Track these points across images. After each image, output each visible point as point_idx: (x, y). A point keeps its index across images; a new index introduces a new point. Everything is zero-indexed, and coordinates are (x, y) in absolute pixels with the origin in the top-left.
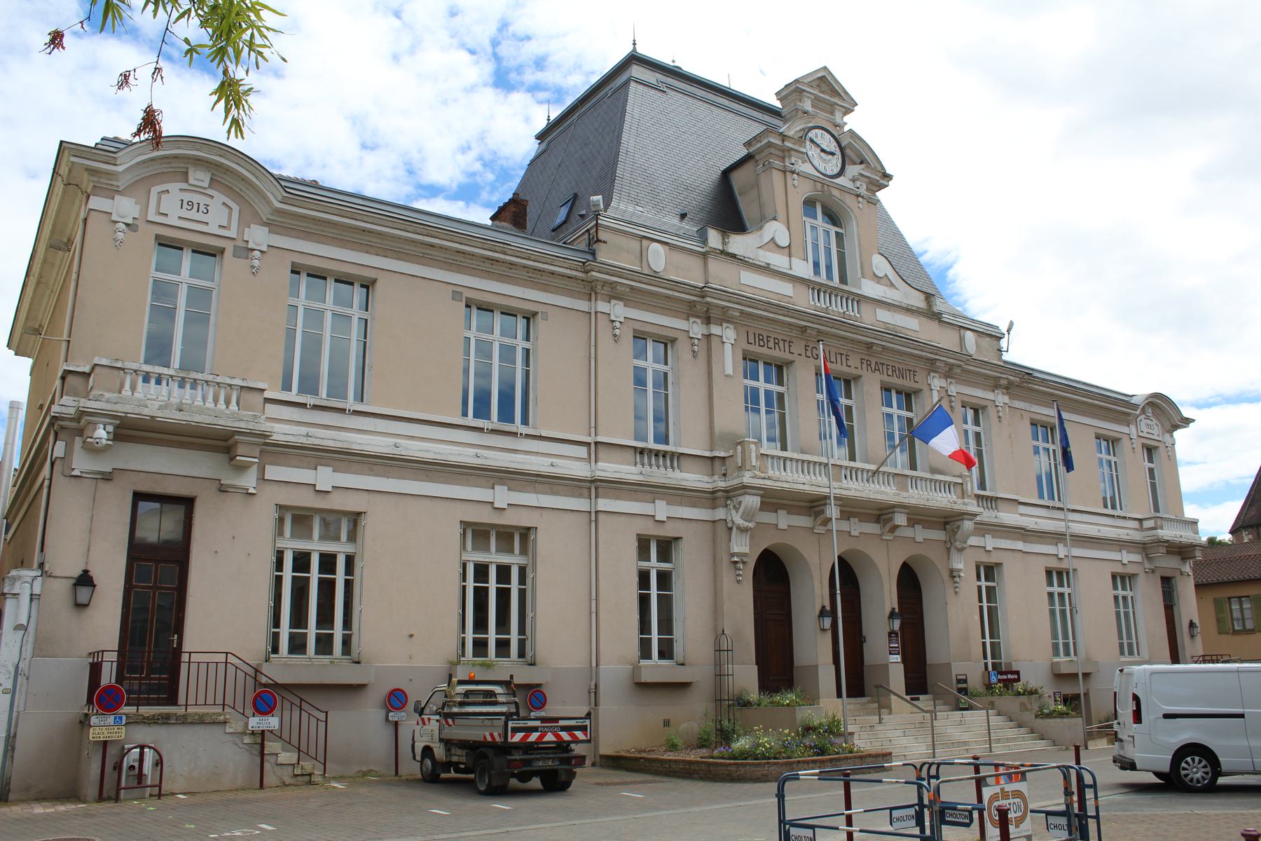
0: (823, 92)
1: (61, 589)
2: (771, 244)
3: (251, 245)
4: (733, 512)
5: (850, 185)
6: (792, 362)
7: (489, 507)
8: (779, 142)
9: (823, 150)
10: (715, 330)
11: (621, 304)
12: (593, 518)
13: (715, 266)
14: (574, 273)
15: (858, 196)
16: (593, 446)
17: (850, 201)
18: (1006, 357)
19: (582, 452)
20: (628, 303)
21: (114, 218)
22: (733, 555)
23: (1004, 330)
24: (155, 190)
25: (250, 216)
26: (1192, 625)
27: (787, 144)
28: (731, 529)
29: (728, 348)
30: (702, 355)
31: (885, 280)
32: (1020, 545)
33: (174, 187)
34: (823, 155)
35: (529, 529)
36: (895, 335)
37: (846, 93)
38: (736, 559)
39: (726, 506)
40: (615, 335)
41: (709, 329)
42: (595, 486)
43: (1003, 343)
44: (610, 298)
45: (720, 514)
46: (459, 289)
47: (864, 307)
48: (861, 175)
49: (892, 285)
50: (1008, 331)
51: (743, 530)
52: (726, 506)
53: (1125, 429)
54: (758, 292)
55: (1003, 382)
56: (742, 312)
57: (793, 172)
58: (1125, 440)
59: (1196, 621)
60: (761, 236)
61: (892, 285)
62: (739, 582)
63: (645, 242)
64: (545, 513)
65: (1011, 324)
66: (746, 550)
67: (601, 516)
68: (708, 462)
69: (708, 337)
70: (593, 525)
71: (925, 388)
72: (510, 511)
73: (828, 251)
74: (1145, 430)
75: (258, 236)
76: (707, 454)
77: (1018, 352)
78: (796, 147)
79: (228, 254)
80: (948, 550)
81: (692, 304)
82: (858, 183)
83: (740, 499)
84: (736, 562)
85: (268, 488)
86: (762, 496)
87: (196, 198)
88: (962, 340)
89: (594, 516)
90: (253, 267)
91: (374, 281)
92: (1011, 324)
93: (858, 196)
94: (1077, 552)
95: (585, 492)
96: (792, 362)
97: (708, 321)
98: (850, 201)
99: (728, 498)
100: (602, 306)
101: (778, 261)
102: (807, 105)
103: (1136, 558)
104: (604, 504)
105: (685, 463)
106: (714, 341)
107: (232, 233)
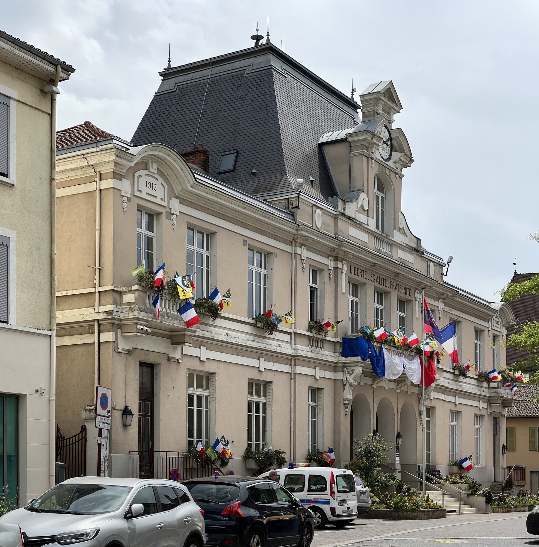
1: (117, 415)
3: (173, 212)
4: (348, 375)
6: (365, 284)
7: (257, 370)
10: (340, 265)
11: (305, 248)
12: (293, 377)
13: (342, 224)
14: (291, 230)
16: (293, 334)
18: (445, 278)
19: (287, 338)
20: (309, 249)
21: (123, 194)
22: (345, 400)
23: (446, 262)
24: (137, 174)
25: (172, 194)
26: (504, 446)
28: (344, 385)
29: (344, 275)
30: (333, 279)
32: (443, 396)
33: (143, 172)
35: (267, 382)
36: (403, 265)
38: (347, 402)
39: (343, 371)
40: (303, 268)
41: (337, 264)
42: (293, 360)
43: (444, 270)
44: (302, 245)
45: (340, 375)
46: (246, 239)
47: (394, 248)
50: (449, 262)
51: (351, 385)
52: (343, 371)
53: (485, 324)
54: (357, 241)
55: (445, 296)
56: (353, 255)
58: (486, 332)
59: (505, 445)
60: (357, 204)
62: (346, 415)
63: (314, 208)
64: (276, 374)
65: (451, 258)
66: (351, 398)
67: (297, 376)
68: (333, 344)
69: (336, 268)
70: (293, 380)
71: (414, 299)
72: (269, 373)
73: (378, 208)
74: (495, 325)
75: (176, 206)
76: (334, 340)
77: (453, 278)
79: (164, 216)
80: (419, 399)
81: (334, 249)
83: (353, 368)
84: (346, 404)
85: (186, 359)
86: (363, 367)
87: (153, 181)
88: (428, 267)
89: (293, 376)
90: (173, 225)
91: (215, 233)
92: (451, 258)
94: (463, 401)
95: (289, 361)
96: (365, 284)
97: (336, 259)
99: (343, 367)
100: (299, 250)
101: (362, 218)
103: (485, 405)
104: (300, 369)
105: (326, 345)
106: (339, 270)
107: (165, 204)
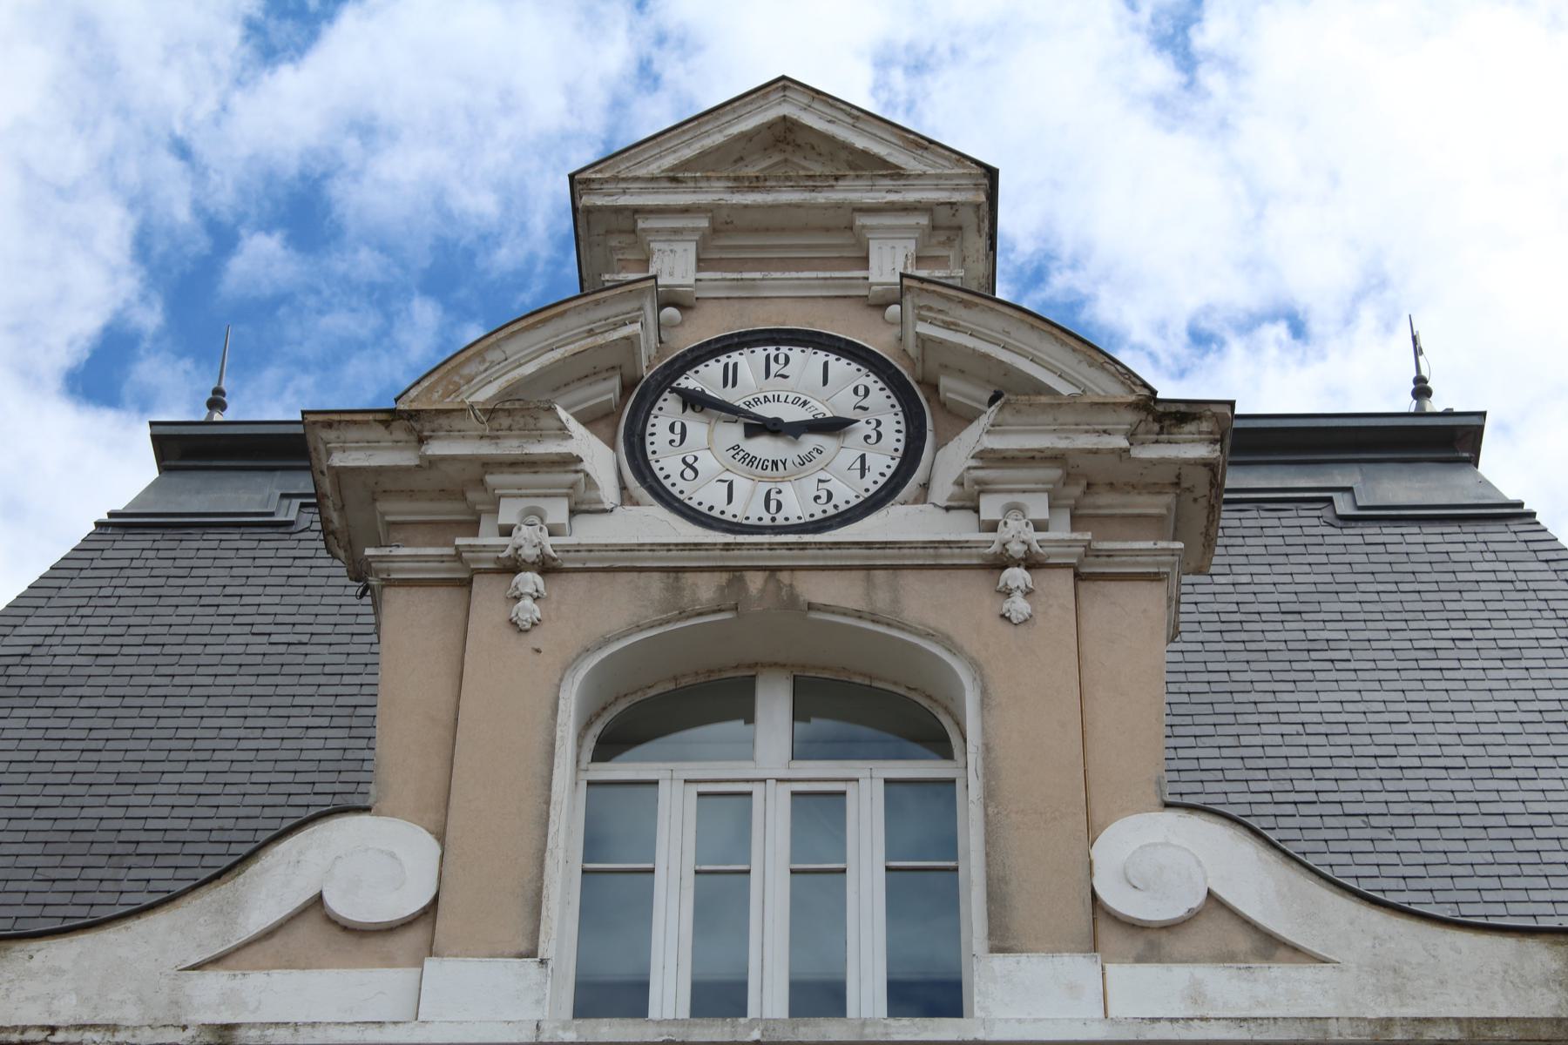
0: (756, 183)
2: (309, 930)
5: (960, 528)
8: (404, 458)
9: (759, 427)
15: (999, 563)
17: (922, 602)
27: (436, 449)
31: (1216, 930)
34: (764, 447)
37: (922, 144)
48: (987, 458)
49: (1270, 945)
57: (512, 567)
61: (1270, 945)
78: (510, 447)
82: (991, 507)
93: (999, 563)
98: (922, 602)
102: (676, 265)
